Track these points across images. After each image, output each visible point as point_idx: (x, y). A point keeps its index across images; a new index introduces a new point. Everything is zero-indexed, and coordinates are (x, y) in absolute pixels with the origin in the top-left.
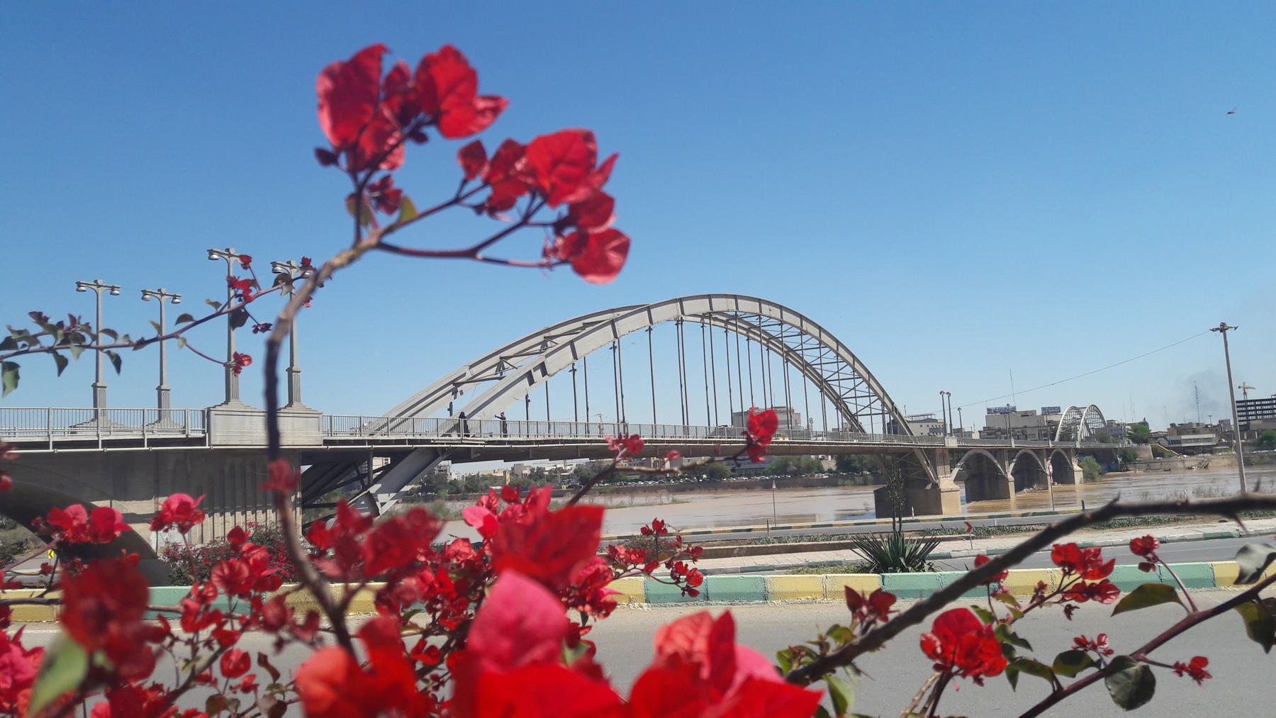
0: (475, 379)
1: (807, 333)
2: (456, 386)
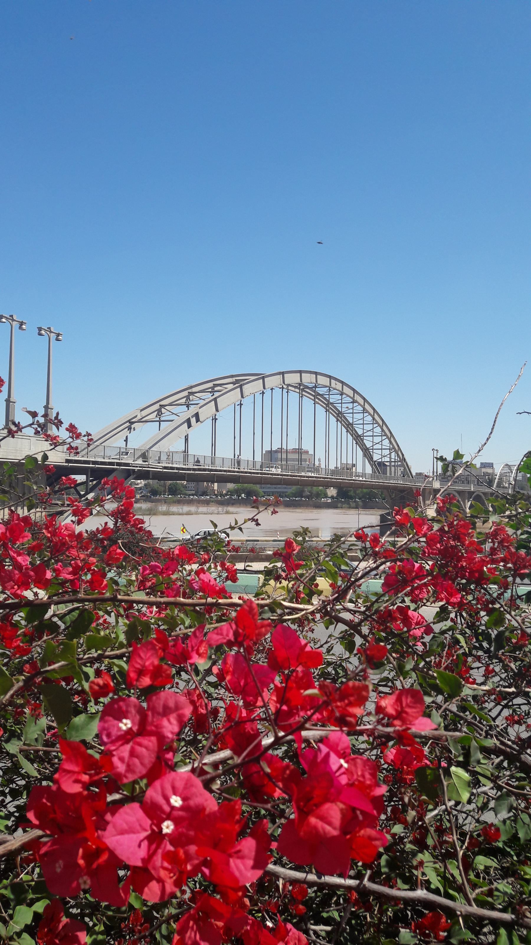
0: (144, 419)
1: (356, 402)
2: (130, 424)
